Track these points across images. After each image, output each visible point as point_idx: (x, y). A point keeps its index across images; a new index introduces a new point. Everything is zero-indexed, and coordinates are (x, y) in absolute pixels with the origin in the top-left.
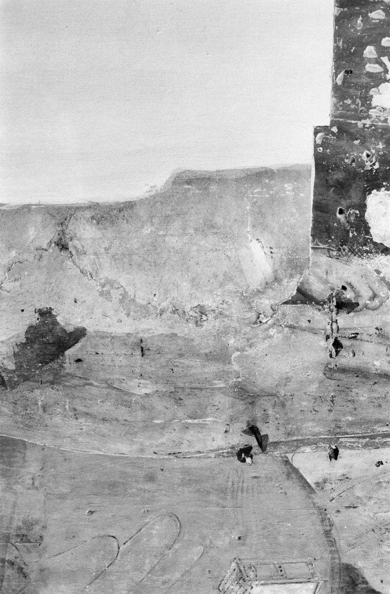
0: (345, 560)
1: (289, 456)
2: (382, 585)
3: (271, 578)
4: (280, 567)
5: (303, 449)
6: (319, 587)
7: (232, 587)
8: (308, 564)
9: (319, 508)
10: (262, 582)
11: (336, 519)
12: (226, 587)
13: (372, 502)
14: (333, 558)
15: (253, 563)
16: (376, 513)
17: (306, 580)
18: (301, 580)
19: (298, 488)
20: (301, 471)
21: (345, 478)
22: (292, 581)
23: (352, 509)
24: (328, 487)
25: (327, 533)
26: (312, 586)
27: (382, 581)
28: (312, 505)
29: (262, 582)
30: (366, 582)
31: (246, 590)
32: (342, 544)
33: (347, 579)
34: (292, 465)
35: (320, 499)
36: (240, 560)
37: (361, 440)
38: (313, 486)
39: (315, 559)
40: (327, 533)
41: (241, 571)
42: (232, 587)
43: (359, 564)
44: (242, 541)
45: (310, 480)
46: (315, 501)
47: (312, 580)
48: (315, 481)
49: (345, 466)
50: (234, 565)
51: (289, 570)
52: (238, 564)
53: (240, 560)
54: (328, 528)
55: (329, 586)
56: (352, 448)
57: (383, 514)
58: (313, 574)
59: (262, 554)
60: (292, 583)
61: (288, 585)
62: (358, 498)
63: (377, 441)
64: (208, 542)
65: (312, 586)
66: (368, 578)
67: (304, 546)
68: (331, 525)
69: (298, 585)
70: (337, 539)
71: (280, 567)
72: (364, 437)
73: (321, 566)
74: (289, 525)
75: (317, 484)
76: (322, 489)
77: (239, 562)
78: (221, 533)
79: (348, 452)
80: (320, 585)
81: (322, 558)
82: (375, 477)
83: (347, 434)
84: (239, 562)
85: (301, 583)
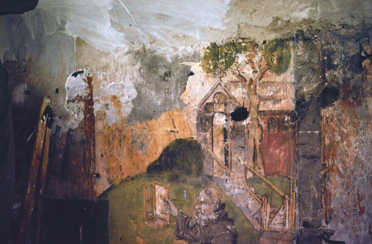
0: (145, 171)
1: (97, 195)
2: (157, 153)
3: (152, 206)
4: (147, 201)
5: (95, 189)
6: (158, 183)
7: (156, 224)
8: (146, 188)
9: (121, 183)
10: (154, 209)
11: (125, 176)
12: (157, 227)
13: (119, 158)
14: (144, 176)
15: (145, 213)
16: (124, 156)
17: (154, 189)
18: (154, 192)
19: (112, 192)
20: (104, 190)
21: (108, 171)
22: (154, 195)
23: (122, 167)
24: (111, 178)
25: (133, 179)
26: (157, 187)
27: (156, 154)
28: (120, 186)
29: (154, 209)
30: (155, 161)
31: (158, 217)
32: (137, 172)
33: (154, 170)
34: (102, 194)
35: (117, 182)
36: (143, 220)
37: (92, 164)
38: (111, 185)
39: (144, 185)
40: (133, 179)
41: (149, 219)
42: (156, 224)
43: (147, 164)
44: (135, 218)
45: (108, 186)
46: (117, 184)
47: (154, 186)
48: (109, 184)
49: (103, 171)
50: (146, 223)
51: (149, 197)
52: (145, 221)
53: (143, 220)
54: (130, 178)
55: (157, 178)
56: (95, 168)
57: (125, 154)
58: (151, 186)
59: (140, 210)
60: (155, 195)
61: (156, 197)
62: (117, 165)
63: (92, 157)
64: (135, 234)
65: (157, 187)
66: (155, 160)
67: (138, 189)
68: (129, 177)
69: (156, 193)
70: (135, 174)
71: (147, 201)
72: (91, 162)
73: (147, 183)
74: (128, 196)
75: (110, 183)
76: (112, 181)
77: (144, 220)
78: (131, 227)
79: (97, 170)
80: (156, 182)
81: (144, 181)
82: (108, 157)
83: (89, 170)
84: (144, 220)
85: (155, 191)
